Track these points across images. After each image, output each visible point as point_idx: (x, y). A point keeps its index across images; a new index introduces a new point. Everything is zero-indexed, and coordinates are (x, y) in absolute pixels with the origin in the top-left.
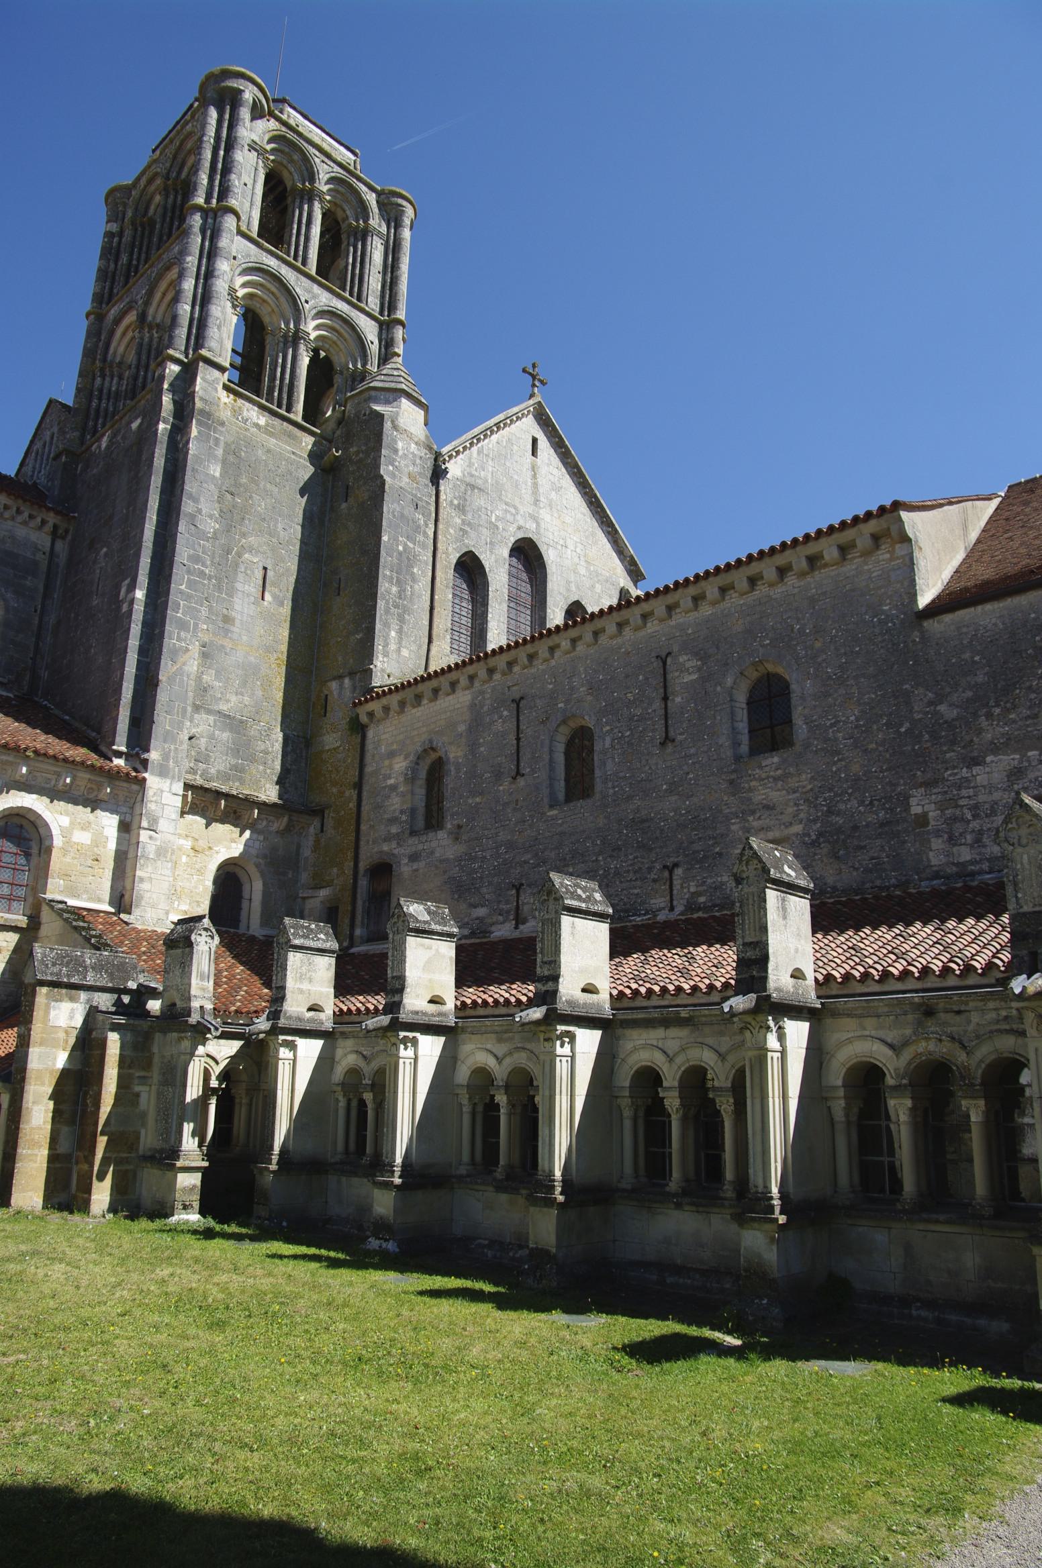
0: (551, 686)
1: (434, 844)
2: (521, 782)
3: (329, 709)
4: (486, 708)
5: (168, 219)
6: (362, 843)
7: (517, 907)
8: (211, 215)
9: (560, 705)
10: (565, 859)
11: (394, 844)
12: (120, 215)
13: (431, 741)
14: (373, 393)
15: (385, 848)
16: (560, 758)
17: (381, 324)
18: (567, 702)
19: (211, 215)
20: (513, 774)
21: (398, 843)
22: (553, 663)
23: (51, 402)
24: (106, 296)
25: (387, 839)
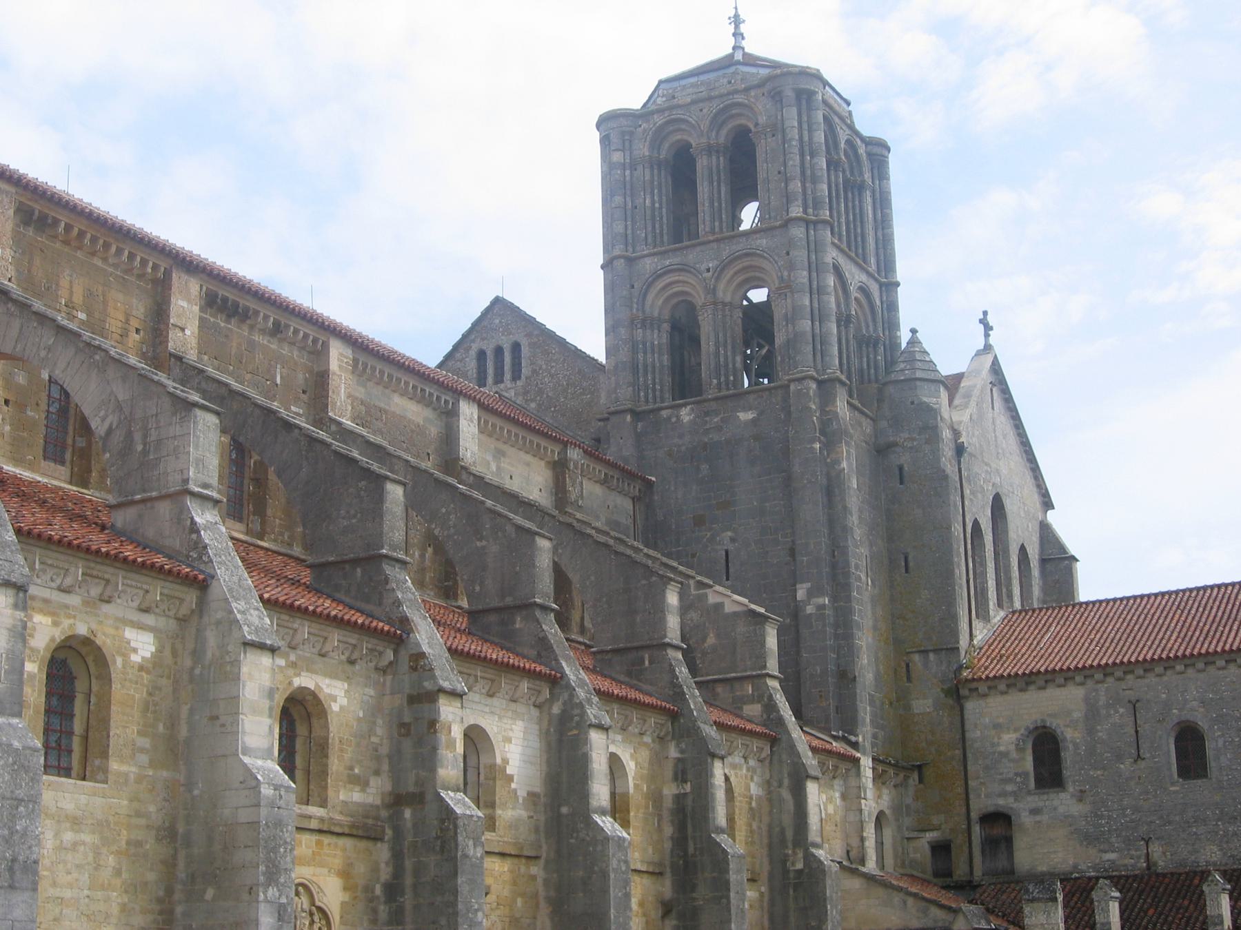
0: (1164, 696)
1: (1056, 803)
2: (1142, 764)
3: (913, 675)
4: (1101, 703)
5: (715, 184)
6: (971, 796)
7: (1148, 854)
8: (812, 227)
9: (1175, 711)
10: (1188, 822)
11: (1011, 800)
12: (627, 144)
13: (1043, 721)
14: (918, 383)
15: (1001, 802)
16: (1172, 747)
17: (881, 285)
18: (1180, 710)
19: (812, 227)
20: (1135, 756)
21: (1015, 800)
22: (1165, 678)
23: (497, 301)
24: (630, 237)
25: (1004, 794)
